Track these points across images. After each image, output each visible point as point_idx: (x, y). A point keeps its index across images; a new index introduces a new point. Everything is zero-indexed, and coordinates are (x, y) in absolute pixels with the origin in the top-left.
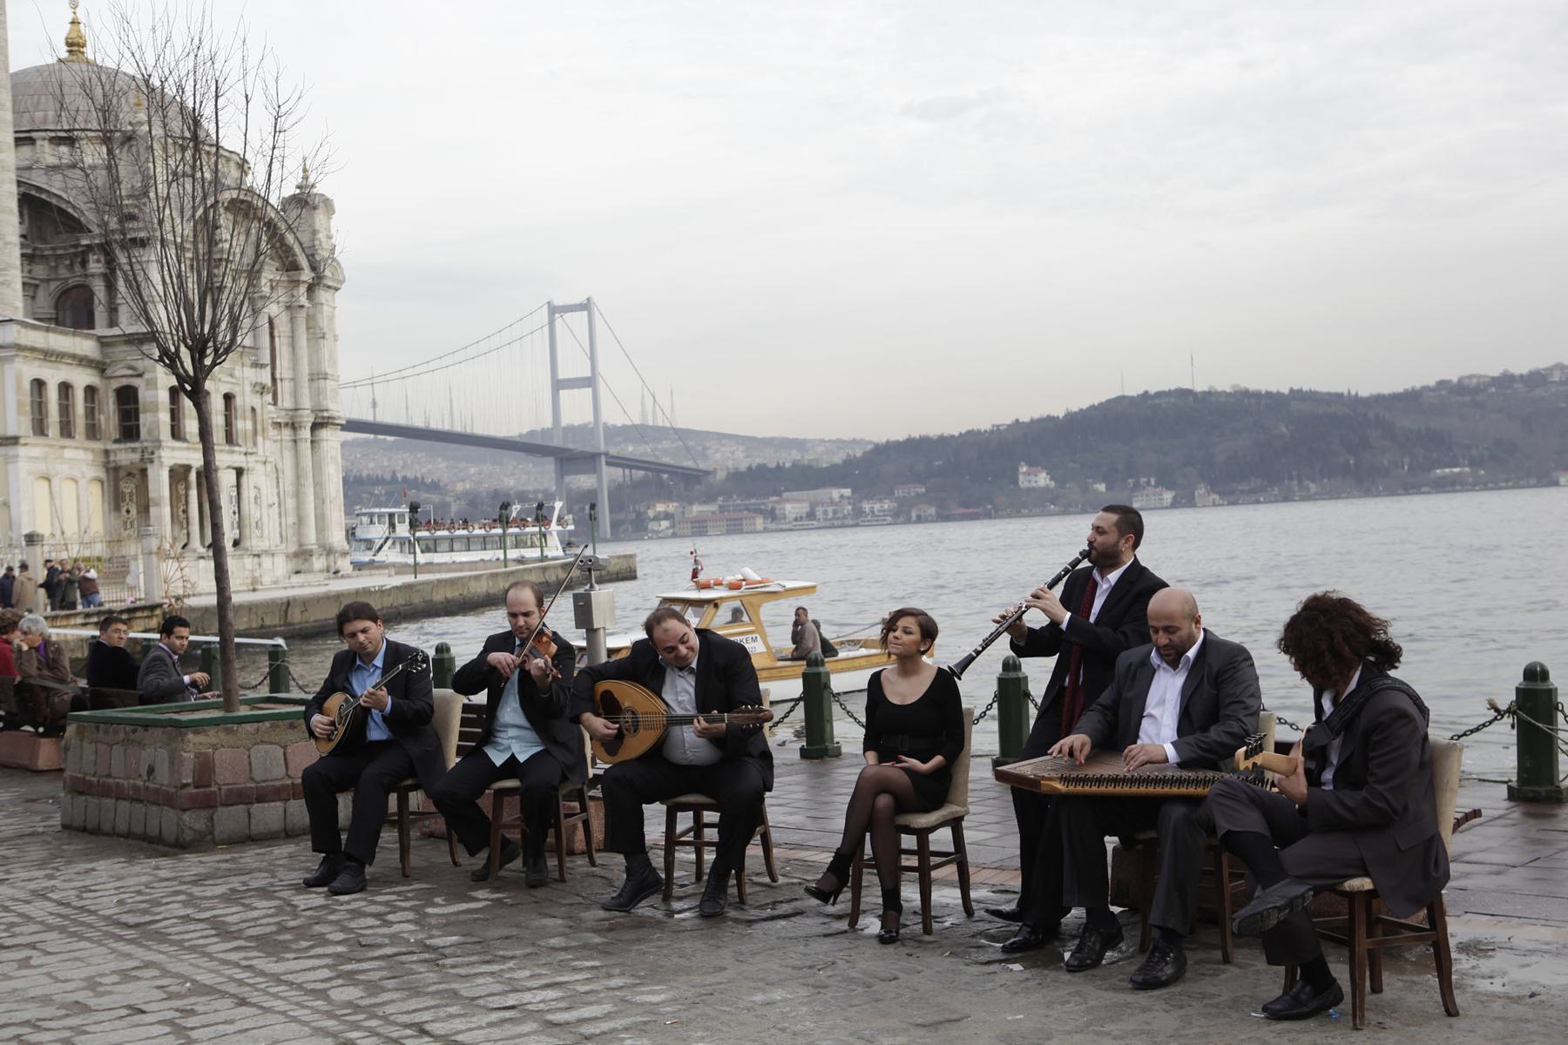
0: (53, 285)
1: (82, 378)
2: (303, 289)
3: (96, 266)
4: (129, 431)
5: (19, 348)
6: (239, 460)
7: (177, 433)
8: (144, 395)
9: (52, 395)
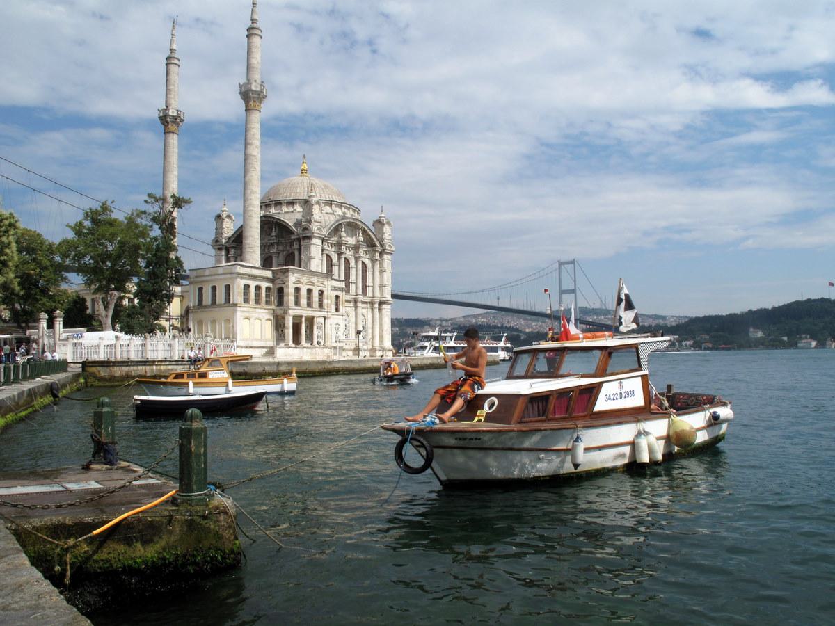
0: (284, 253)
1: (264, 285)
2: (377, 254)
3: (296, 246)
4: (281, 303)
5: (239, 274)
6: (324, 314)
7: (297, 303)
8: (285, 290)
9: (252, 290)
